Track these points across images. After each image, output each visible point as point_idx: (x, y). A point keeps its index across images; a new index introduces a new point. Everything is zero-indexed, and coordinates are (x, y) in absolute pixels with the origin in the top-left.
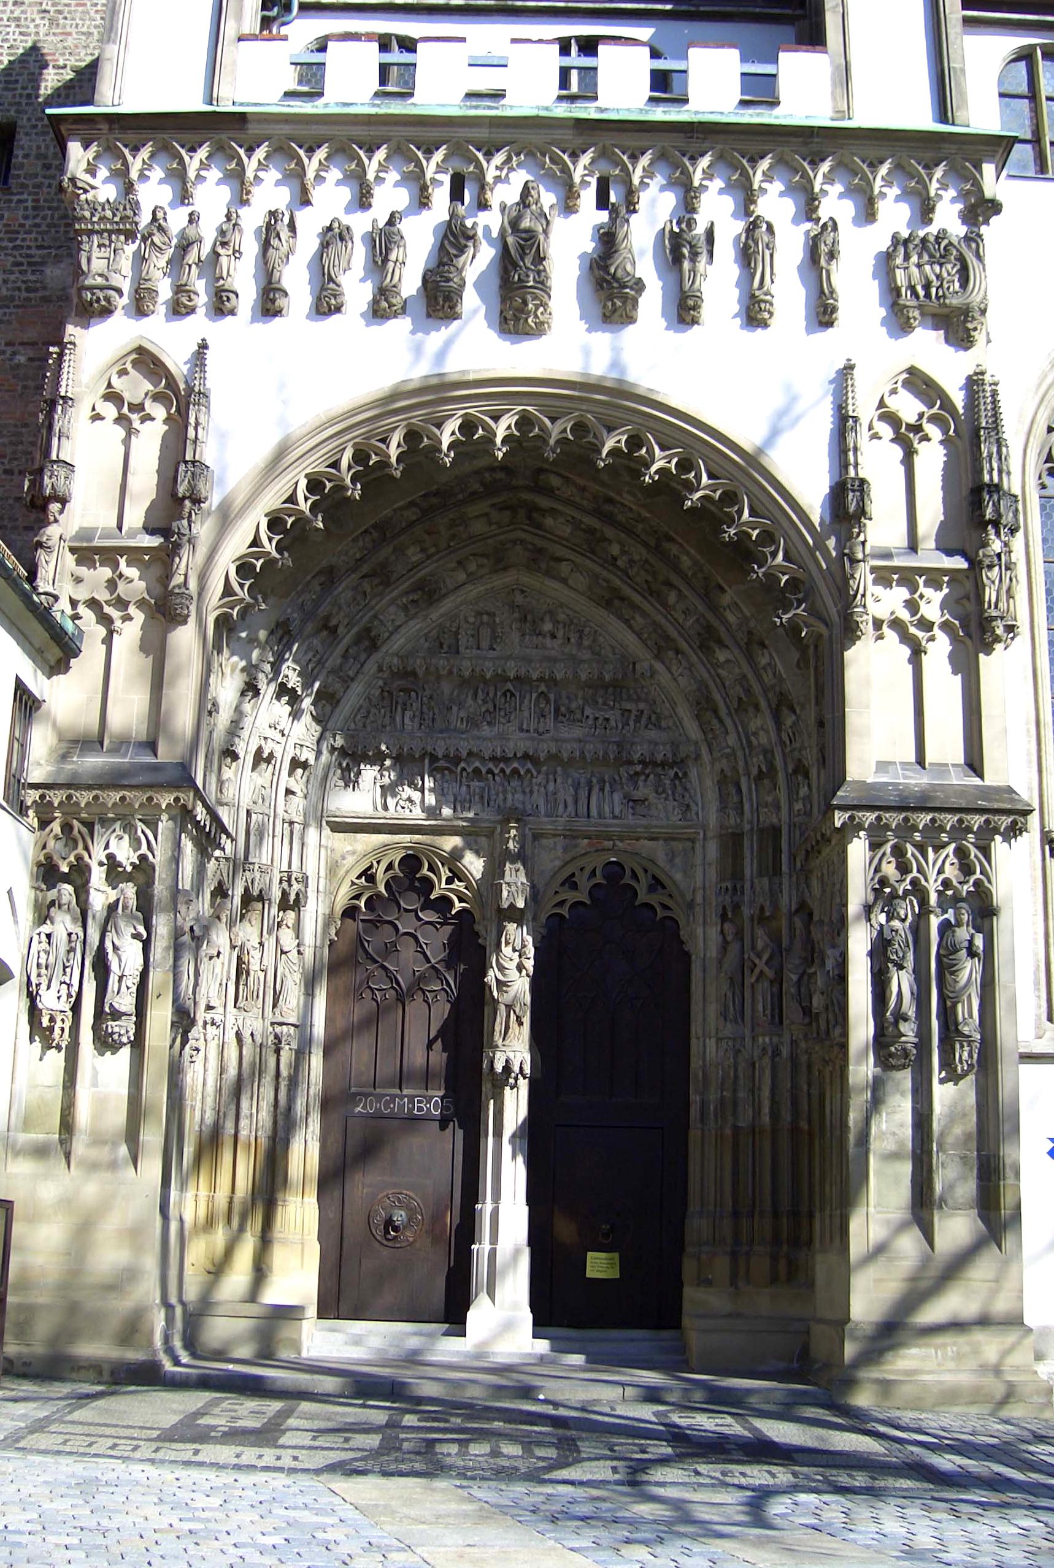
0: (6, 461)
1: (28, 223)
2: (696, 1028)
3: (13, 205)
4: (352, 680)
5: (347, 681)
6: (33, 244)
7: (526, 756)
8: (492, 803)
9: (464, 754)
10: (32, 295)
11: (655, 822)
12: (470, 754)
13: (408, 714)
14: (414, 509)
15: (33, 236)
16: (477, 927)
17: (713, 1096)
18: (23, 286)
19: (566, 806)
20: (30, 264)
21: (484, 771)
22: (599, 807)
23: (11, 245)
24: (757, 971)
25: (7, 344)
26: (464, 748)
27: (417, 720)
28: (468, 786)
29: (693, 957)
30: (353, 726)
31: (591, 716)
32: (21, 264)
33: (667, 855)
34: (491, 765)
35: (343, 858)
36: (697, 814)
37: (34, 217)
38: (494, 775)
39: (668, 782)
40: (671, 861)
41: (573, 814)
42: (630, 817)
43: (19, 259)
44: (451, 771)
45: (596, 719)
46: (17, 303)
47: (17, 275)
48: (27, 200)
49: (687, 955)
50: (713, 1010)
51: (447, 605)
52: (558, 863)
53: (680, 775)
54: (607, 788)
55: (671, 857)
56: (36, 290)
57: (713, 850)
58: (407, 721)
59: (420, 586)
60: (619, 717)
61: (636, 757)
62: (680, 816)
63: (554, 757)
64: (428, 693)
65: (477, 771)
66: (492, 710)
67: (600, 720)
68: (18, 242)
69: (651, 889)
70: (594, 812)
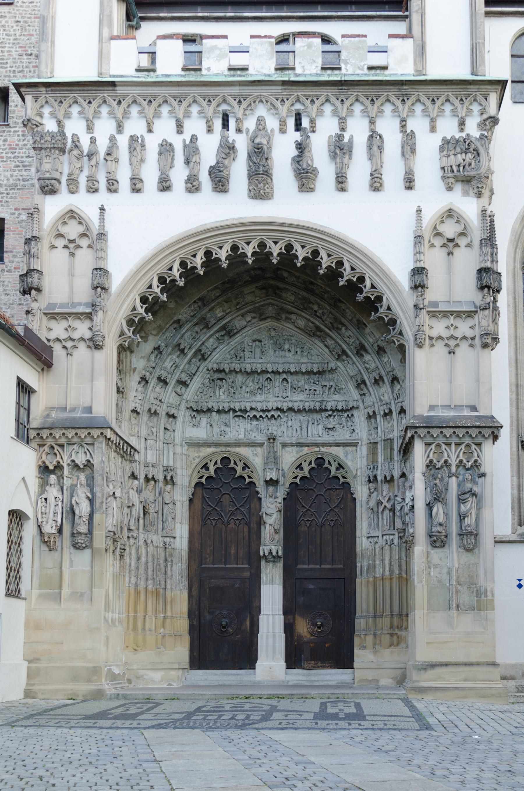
0: (20, 271)
1: (21, 143)
3: (12, 133)
4: (194, 375)
5: (192, 376)
6: (24, 155)
7: (277, 409)
8: (262, 431)
9: (248, 409)
10: (26, 183)
12: (252, 409)
13: (222, 390)
14: (218, 290)
15: (24, 150)
16: (257, 489)
18: (21, 178)
20: (24, 166)
21: (258, 416)
23: (13, 156)
24: (383, 506)
25: (16, 209)
27: (226, 393)
28: (251, 424)
30: (196, 397)
32: (18, 166)
34: (261, 414)
35: (194, 460)
37: (24, 140)
38: (263, 418)
43: (18, 164)
44: (243, 417)
46: (18, 187)
47: (17, 172)
48: (18, 131)
50: (365, 524)
51: (238, 338)
52: (294, 459)
56: (28, 180)
57: (364, 450)
58: (221, 394)
59: (224, 328)
64: (231, 380)
65: (255, 416)
68: (16, 154)
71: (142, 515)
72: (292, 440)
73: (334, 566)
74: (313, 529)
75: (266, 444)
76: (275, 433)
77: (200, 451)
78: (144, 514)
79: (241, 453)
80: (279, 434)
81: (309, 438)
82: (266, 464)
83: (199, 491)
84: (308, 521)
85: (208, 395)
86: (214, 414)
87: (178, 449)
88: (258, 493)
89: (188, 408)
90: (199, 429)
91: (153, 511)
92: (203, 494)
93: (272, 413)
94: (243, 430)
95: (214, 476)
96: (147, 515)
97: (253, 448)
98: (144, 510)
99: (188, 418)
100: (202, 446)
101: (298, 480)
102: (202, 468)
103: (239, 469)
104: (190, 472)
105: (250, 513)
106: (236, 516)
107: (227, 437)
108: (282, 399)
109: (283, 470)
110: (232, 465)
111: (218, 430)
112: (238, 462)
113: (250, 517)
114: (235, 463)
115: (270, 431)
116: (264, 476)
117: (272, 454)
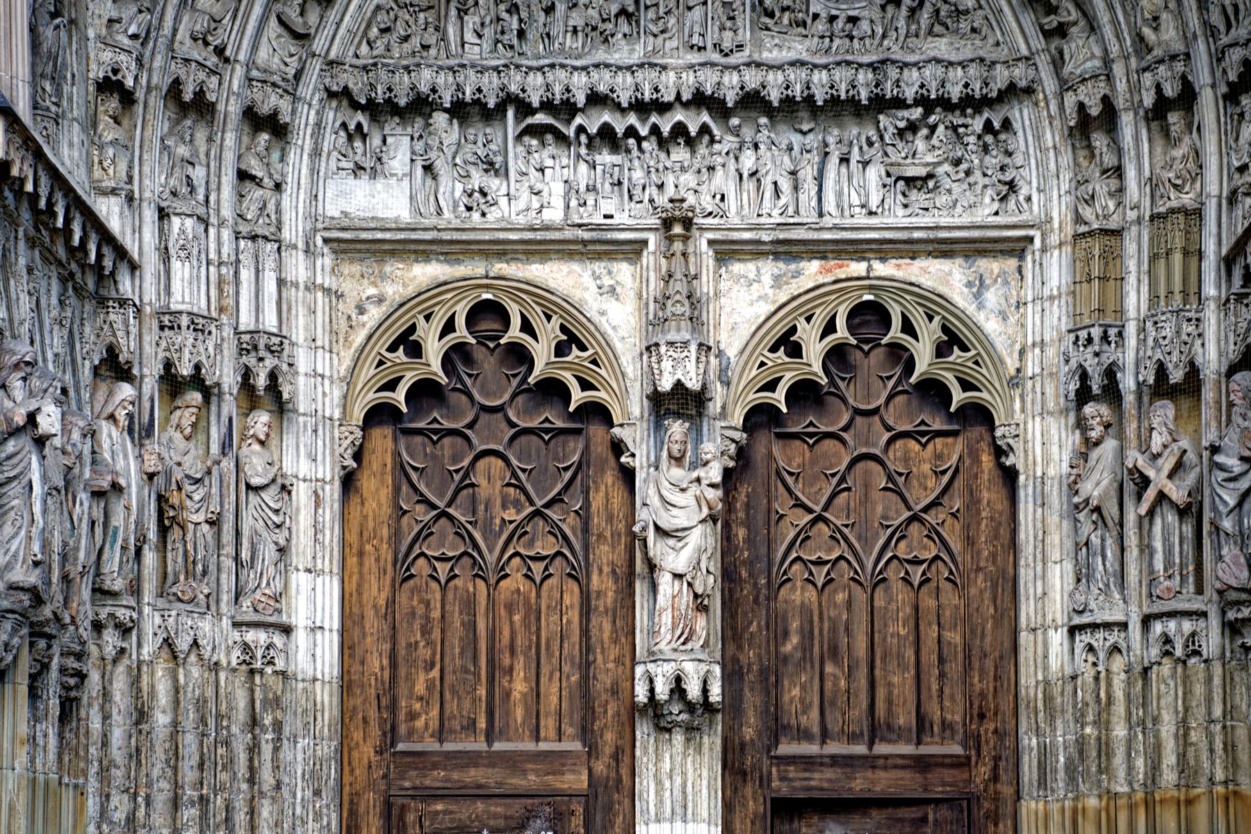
2: (1027, 611)
7: (700, 100)
8: (637, 191)
9: (581, 99)
11: (944, 221)
12: (596, 99)
16: (616, 431)
17: (1062, 736)
19: (777, 192)
21: (620, 129)
22: (839, 194)
26: (580, 86)
27: (488, 32)
29: (1022, 478)
30: (364, 49)
31: (823, 15)
33: (969, 284)
34: (632, 119)
35: (361, 310)
36: (1029, 199)
38: (639, 140)
39: (972, 139)
40: (977, 296)
41: (791, 211)
42: (900, 212)
45: (832, 19)
49: (1010, 476)
50: (1059, 577)
52: (765, 309)
53: (997, 125)
54: (855, 156)
55: (979, 287)
58: (470, 37)
60: (876, 14)
61: (910, 93)
62: (996, 206)
63: (752, 101)
65: (606, 132)
66: (631, 9)
67: (840, 24)
69: (942, 350)
70: (830, 204)
71: (152, 535)
72: (758, 228)
73: (924, 750)
74: (841, 597)
75: (652, 246)
76: (691, 199)
77: (383, 277)
78: (163, 531)
79: (552, 285)
80: (708, 203)
81: (828, 221)
82: (658, 323)
83: (382, 438)
84: (820, 563)
85: (415, 42)
86: (440, 119)
87: (297, 267)
88: (618, 447)
89: (331, 95)
90: (380, 184)
91: (200, 517)
92: (397, 454)
93: (679, 116)
94: (559, 188)
95: (444, 380)
96: (176, 533)
97: (599, 266)
98: (161, 513)
99: (332, 140)
100: (393, 253)
101: (779, 397)
102: (392, 348)
103: (542, 352)
104: (347, 363)
105: (586, 530)
106: (531, 544)
107: (494, 215)
108: (716, 57)
109: (720, 354)
110: (514, 333)
111: (459, 187)
112: (538, 322)
113: (586, 547)
114: (527, 327)
115: (670, 191)
116: (652, 375)
117: (679, 286)
